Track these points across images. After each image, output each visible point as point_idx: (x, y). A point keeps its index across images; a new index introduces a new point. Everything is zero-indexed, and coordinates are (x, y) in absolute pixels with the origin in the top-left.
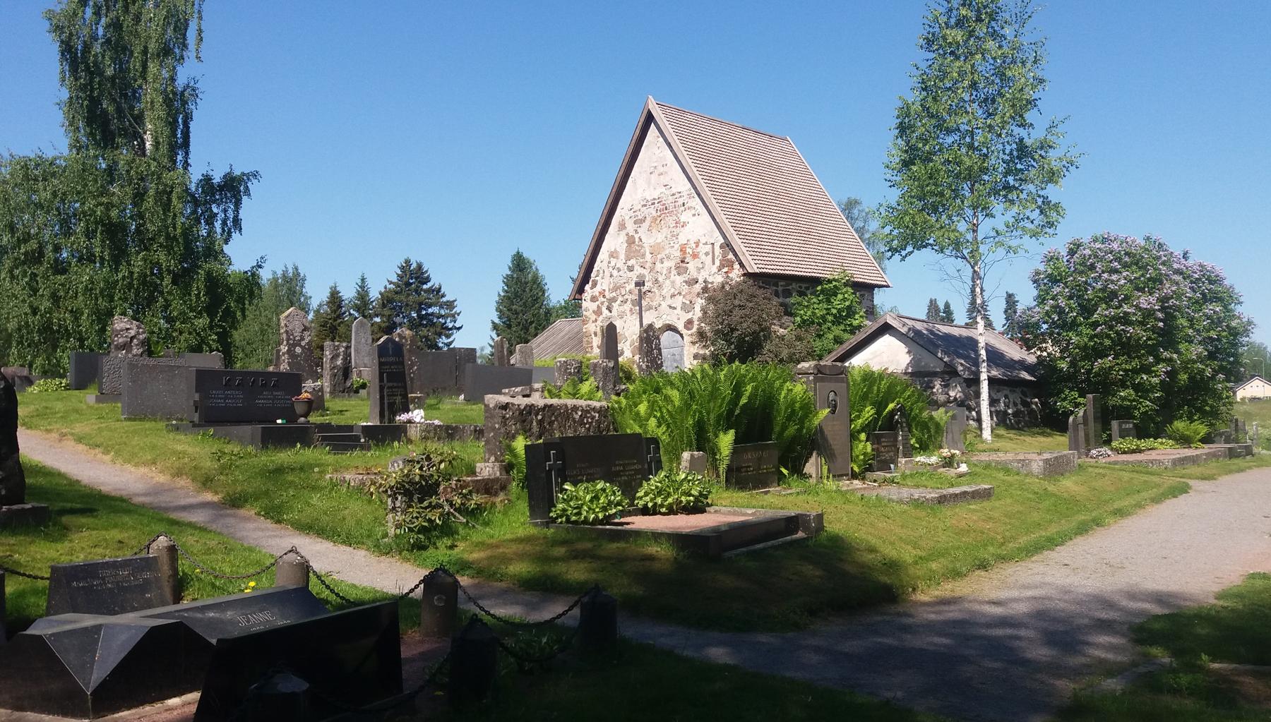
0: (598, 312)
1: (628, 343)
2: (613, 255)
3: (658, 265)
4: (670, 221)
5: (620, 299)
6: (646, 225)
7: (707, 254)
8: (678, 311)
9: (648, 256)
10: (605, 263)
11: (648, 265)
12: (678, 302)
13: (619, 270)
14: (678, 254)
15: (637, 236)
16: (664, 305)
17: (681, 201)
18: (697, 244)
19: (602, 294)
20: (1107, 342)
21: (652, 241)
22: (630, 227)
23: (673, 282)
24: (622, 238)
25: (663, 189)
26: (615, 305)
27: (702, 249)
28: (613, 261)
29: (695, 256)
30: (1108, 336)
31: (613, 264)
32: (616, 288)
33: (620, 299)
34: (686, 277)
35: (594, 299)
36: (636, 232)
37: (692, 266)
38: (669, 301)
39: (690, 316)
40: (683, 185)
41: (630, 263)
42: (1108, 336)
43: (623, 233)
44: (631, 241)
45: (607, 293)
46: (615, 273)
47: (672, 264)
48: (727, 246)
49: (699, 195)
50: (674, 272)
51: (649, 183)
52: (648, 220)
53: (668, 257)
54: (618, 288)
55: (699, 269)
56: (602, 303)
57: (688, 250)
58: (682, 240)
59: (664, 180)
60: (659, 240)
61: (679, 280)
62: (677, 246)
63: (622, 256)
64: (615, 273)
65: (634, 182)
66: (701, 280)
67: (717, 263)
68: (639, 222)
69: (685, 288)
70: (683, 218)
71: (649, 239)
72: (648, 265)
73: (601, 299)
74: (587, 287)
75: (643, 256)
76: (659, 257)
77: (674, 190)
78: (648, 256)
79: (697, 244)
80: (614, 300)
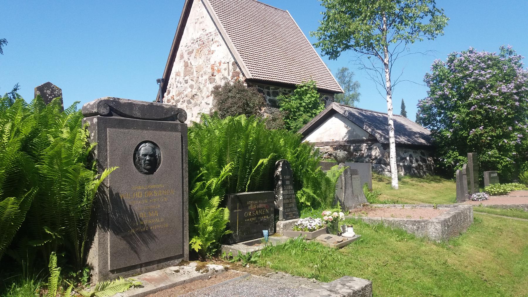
4: (205, 51)
5: (181, 100)
6: (193, 55)
7: (225, 69)
9: (195, 73)
10: (174, 79)
11: (195, 79)
14: (210, 71)
15: (189, 62)
16: (203, 102)
17: (211, 38)
18: (220, 63)
20: (479, 117)
21: (196, 64)
22: (186, 56)
23: (208, 88)
24: (182, 64)
25: (202, 32)
28: (178, 78)
29: (219, 71)
30: (479, 113)
31: (177, 80)
32: (179, 94)
33: (181, 100)
36: (189, 59)
40: (212, 28)
42: (479, 113)
44: (186, 65)
45: (175, 97)
46: (179, 85)
47: (206, 77)
48: (236, 63)
49: (220, 33)
50: (208, 82)
51: (195, 29)
52: (195, 51)
53: (205, 73)
57: (216, 68)
58: (212, 62)
59: (202, 26)
60: (200, 63)
62: (209, 66)
63: (182, 75)
64: (179, 85)
65: (187, 30)
68: (190, 53)
70: (212, 48)
71: (196, 62)
72: (195, 79)
74: (165, 94)
76: (201, 73)
77: (207, 32)
78: (195, 73)
79: (220, 63)
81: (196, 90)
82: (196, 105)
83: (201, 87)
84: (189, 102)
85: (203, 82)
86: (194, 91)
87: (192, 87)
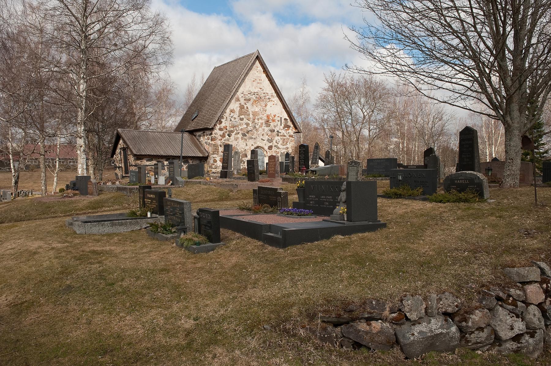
0: (223, 136)
2: (232, 111)
3: (256, 121)
5: (236, 132)
7: (278, 121)
9: (251, 116)
12: (266, 138)
13: (235, 118)
14: (266, 118)
15: (245, 106)
17: (268, 97)
19: (226, 127)
21: (253, 110)
22: (242, 101)
23: (264, 129)
26: (233, 134)
27: (277, 119)
29: (274, 121)
33: (236, 132)
34: (270, 128)
35: (220, 129)
37: (272, 124)
38: (262, 137)
39: (271, 144)
41: (242, 117)
43: (238, 103)
44: (242, 107)
45: (228, 128)
47: (263, 121)
50: (264, 125)
51: (252, 86)
52: (252, 100)
54: (236, 126)
55: (275, 126)
56: (226, 132)
58: (268, 113)
61: (267, 129)
62: (265, 115)
64: (232, 119)
66: (276, 131)
67: (283, 125)
69: (270, 133)
71: (252, 108)
73: (225, 130)
75: (249, 115)
78: (251, 116)
79: (275, 116)
80: (232, 131)
81: (252, 128)
82: (251, 138)
83: (257, 127)
84: (244, 135)
85: (259, 124)
86: (249, 128)
87: (247, 124)
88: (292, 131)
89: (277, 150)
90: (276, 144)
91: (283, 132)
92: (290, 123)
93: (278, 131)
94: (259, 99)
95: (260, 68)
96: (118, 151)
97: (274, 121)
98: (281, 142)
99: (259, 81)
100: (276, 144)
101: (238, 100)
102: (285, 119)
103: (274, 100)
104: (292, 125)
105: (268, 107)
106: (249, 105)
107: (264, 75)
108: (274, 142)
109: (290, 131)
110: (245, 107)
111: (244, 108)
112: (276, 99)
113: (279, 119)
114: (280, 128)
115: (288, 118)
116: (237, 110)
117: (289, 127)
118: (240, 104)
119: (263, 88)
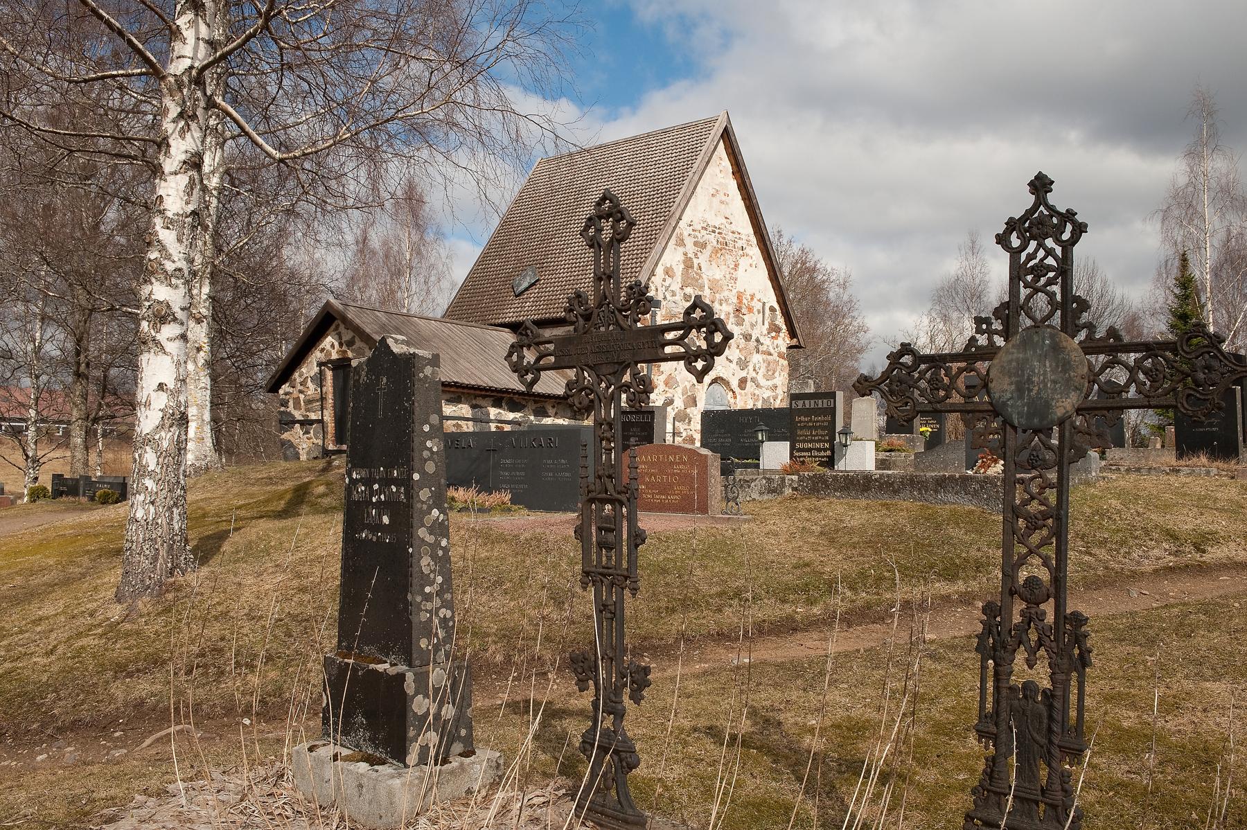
1: (679, 390)
8: (734, 365)
13: (674, 294)
14: (735, 301)
17: (740, 244)
18: (752, 297)
22: (690, 248)
25: (724, 221)
31: (667, 284)
39: (743, 374)
43: (681, 250)
44: (688, 264)
51: (711, 207)
52: (709, 247)
55: (752, 325)
57: (745, 301)
58: (740, 287)
60: (717, 277)
62: (734, 291)
66: (754, 338)
68: (703, 246)
88: (783, 341)
89: (757, 392)
90: (754, 374)
91: (766, 341)
92: (780, 321)
93: (758, 340)
94: (723, 247)
95: (726, 164)
96: (309, 368)
97: (750, 310)
98: (762, 371)
99: (724, 198)
100: (754, 374)
101: (681, 243)
102: (772, 309)
103: (751, 253)
104: (784, 327)
105: (740, 273)
106: (703, 259)
107: (733, 184)
108: (751, 368)
109: (780, 341)
110: (696, 266)
111: (692, 267)
112: (755, 252)
113: (759, 306)
114: (760, 331)
115: (777, 306)
116: (679, 269)
117: (778, 330)
118: (685, 254)
119: (732, 220)
